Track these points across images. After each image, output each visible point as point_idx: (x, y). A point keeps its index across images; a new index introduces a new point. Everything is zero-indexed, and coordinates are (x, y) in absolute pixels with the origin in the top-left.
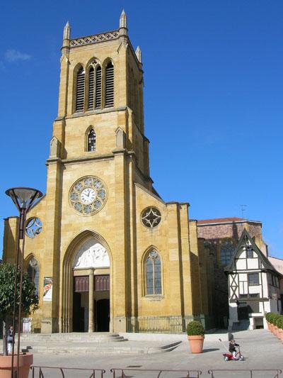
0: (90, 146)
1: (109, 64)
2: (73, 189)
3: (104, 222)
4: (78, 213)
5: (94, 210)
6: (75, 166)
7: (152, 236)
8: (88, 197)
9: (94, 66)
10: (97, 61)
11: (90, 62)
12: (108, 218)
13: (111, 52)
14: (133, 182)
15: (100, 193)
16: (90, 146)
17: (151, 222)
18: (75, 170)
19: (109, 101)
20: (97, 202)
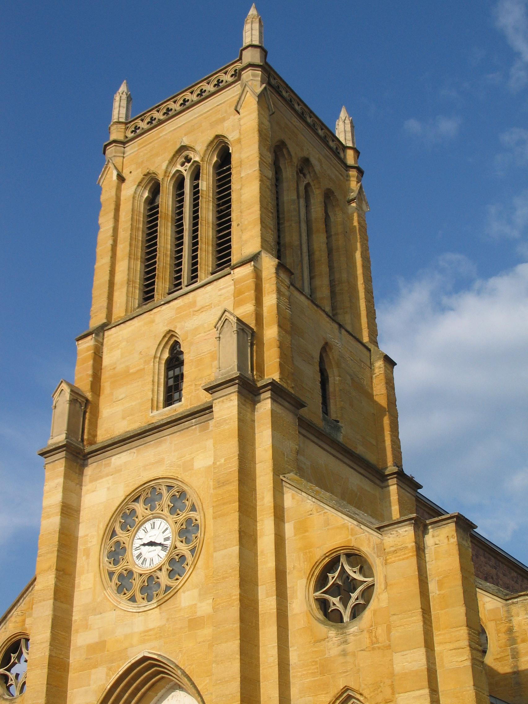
0: (172, 391)
1: (225, 157)
2: (114, 533)
3: (194, 623)
4: (126, 605)
5: (168, 588)
6: (120, 459)
7: (344, 653)
8: (152, 541)
9: (186, 171)
10: (191, 155)
11: (172, 162)
12: (205, 608)
13: (223, 120)
14: (278, 471)
15: (187, 531)
16: (172, 391)
17: (345, 602)
18: (118, 470)
19: (223, 258)
20: (176, 565)
